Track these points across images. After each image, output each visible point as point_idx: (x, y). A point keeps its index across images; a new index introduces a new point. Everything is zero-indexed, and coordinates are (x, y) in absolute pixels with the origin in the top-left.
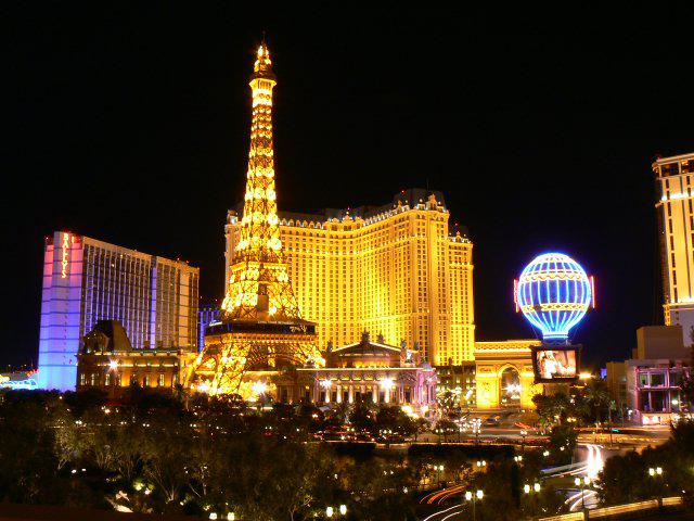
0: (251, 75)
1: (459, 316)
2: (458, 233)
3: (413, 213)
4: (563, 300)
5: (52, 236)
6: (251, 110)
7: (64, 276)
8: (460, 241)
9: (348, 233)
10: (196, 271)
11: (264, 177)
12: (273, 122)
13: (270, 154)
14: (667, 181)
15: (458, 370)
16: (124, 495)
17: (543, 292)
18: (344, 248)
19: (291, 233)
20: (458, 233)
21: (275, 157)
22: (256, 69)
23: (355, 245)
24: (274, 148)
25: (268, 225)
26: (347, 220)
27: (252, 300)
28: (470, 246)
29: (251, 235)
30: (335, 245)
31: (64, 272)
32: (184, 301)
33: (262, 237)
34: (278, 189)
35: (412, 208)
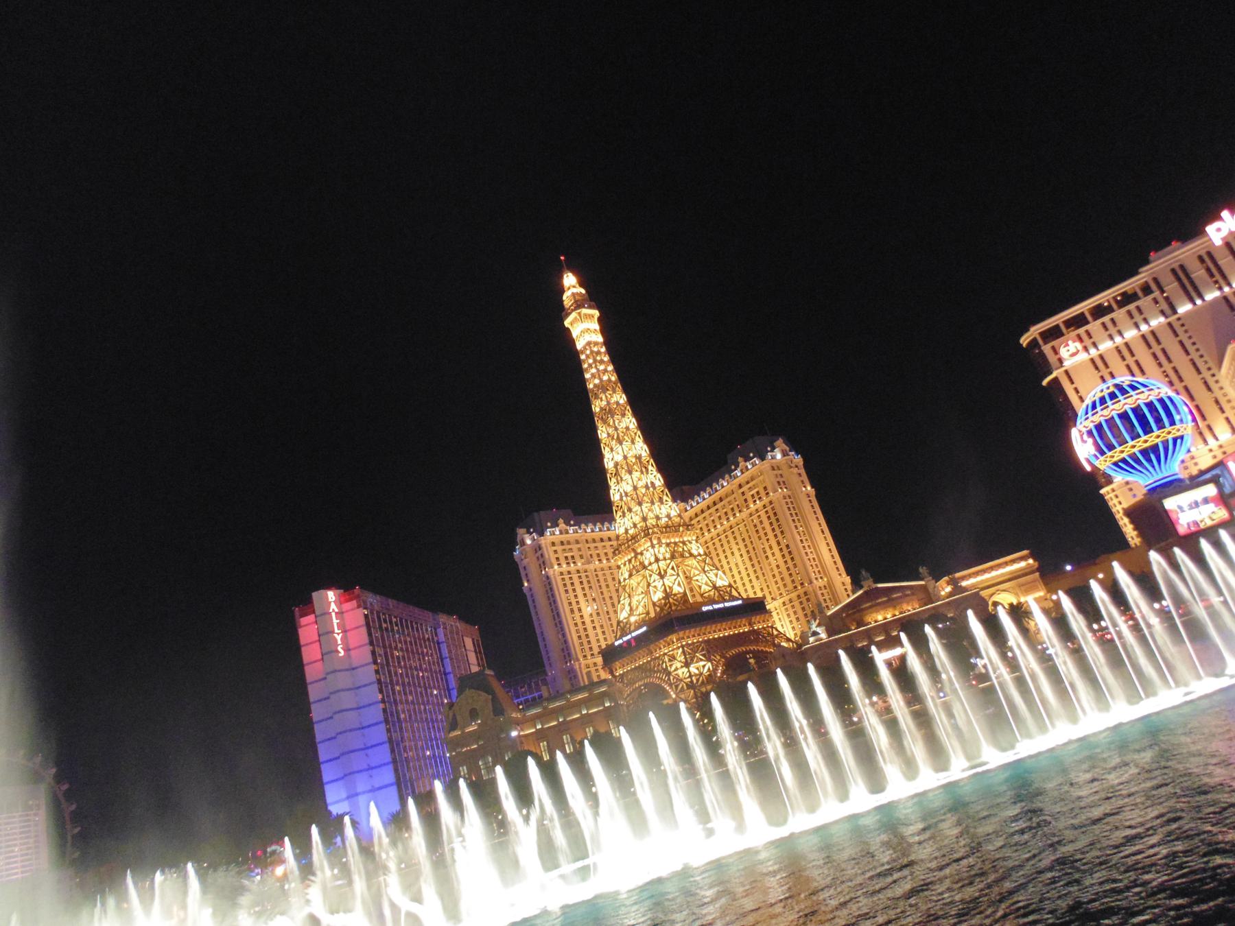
3: (766, 464)
4: (1160, 424)
7: (342, 653)
11: (627, 428)
12: (613, 360)
14: (1053, 348)
19: (602, 540)
21: (631, 401)
24: (625, 391)
29: (640, 504)
31: (339, 648)
33: (653, 503)
34: (647, 440)
35: (763, 458)
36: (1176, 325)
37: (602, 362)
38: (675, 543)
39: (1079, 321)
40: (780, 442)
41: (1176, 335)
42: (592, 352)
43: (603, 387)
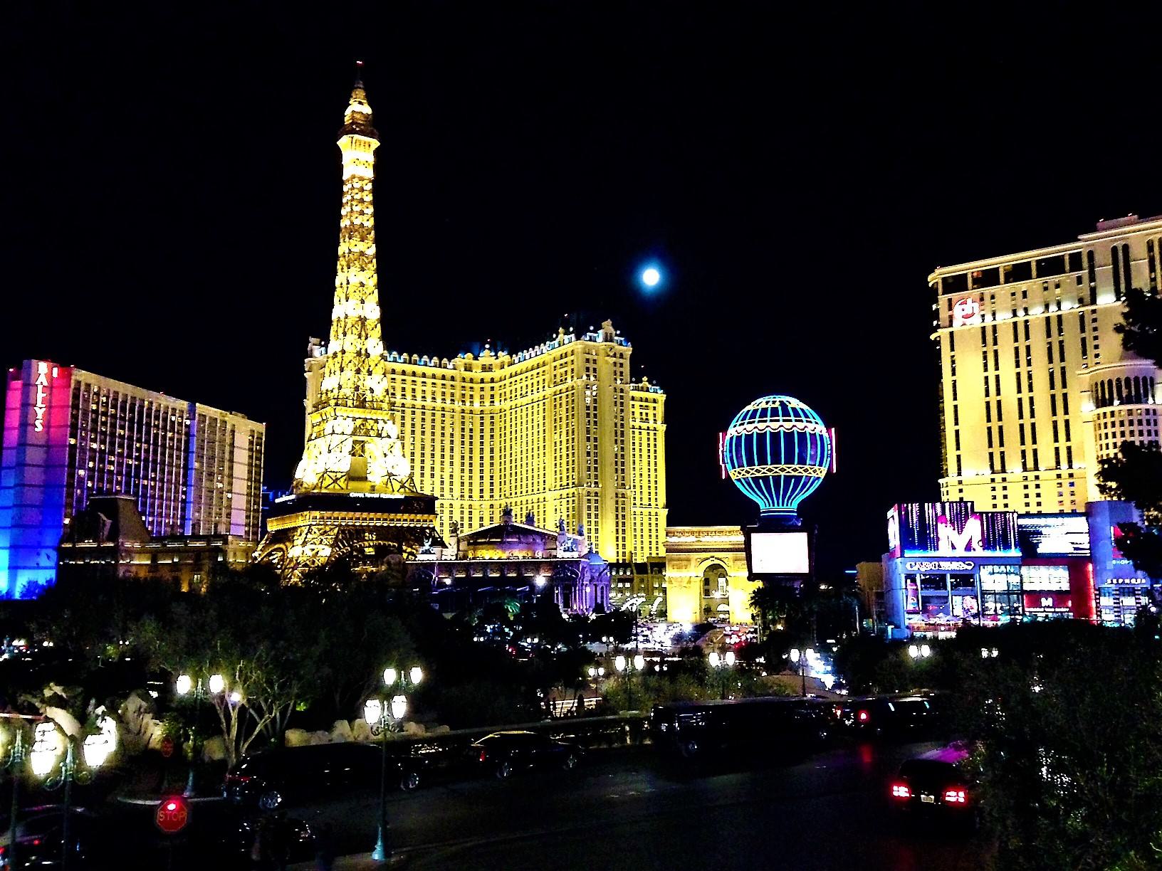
0: (340, 129)
1: (645, 496)
2: (645, 379)
3: (578, 346)
5: (19, 367)
6: (342, 183)
7: (39, 428)
8: (648, 390)
9: (487, 376)
10: (261, 427)
11: (362, 285)
12: (375, 203)
13: (372, 251)
14: (950, 300)
15: (641, 568)
16: (58, 690)
17: (757, 449)
18: (482, 397)
20: (645, 379)
21: (378, 255)
22: (347, 120)
23: (497, 393)
25: (368, 355)
26: (486, 357)
27: (343, 463)
28: (661, 397)
29: (342, 370)
30: (468, 393)
31: (37, 423)
32: (241, 471)
33: (358, 372)
34: (382, 303)
35: (578, 338)
36: (1088, 320)
37: (362, 201)
38: (366, 419)
39: (989, 278)
40: (607, 325)
41: (1083, 330)
42: (353, 188)
43: (352, 231)
